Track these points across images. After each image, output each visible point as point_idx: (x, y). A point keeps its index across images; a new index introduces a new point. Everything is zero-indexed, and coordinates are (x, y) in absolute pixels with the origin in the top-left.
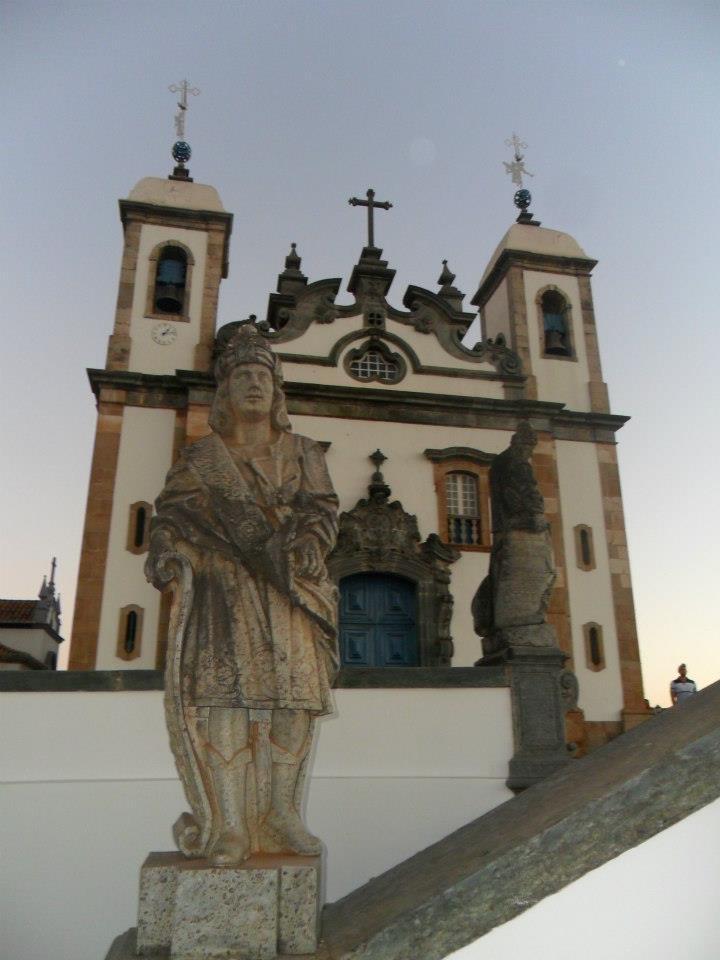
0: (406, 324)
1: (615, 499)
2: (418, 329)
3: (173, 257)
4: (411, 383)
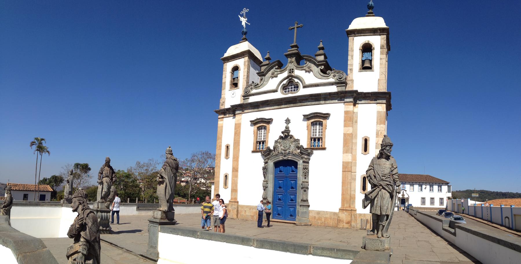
0: (302, 70)
2: (306, 71)
4: (302, 92)
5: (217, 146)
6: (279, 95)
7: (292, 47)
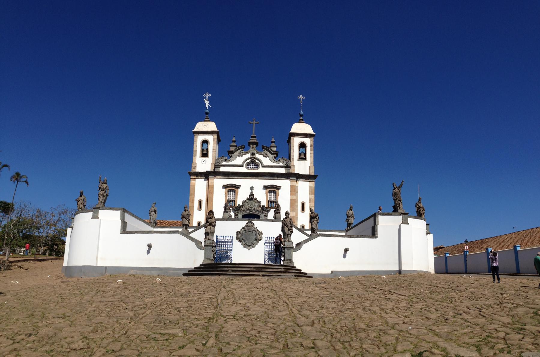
1: (312, 195)
2: (264, 156)
4: (261, 170)
5: (190, 200)
6: (244, 170)
7: (252, 137)
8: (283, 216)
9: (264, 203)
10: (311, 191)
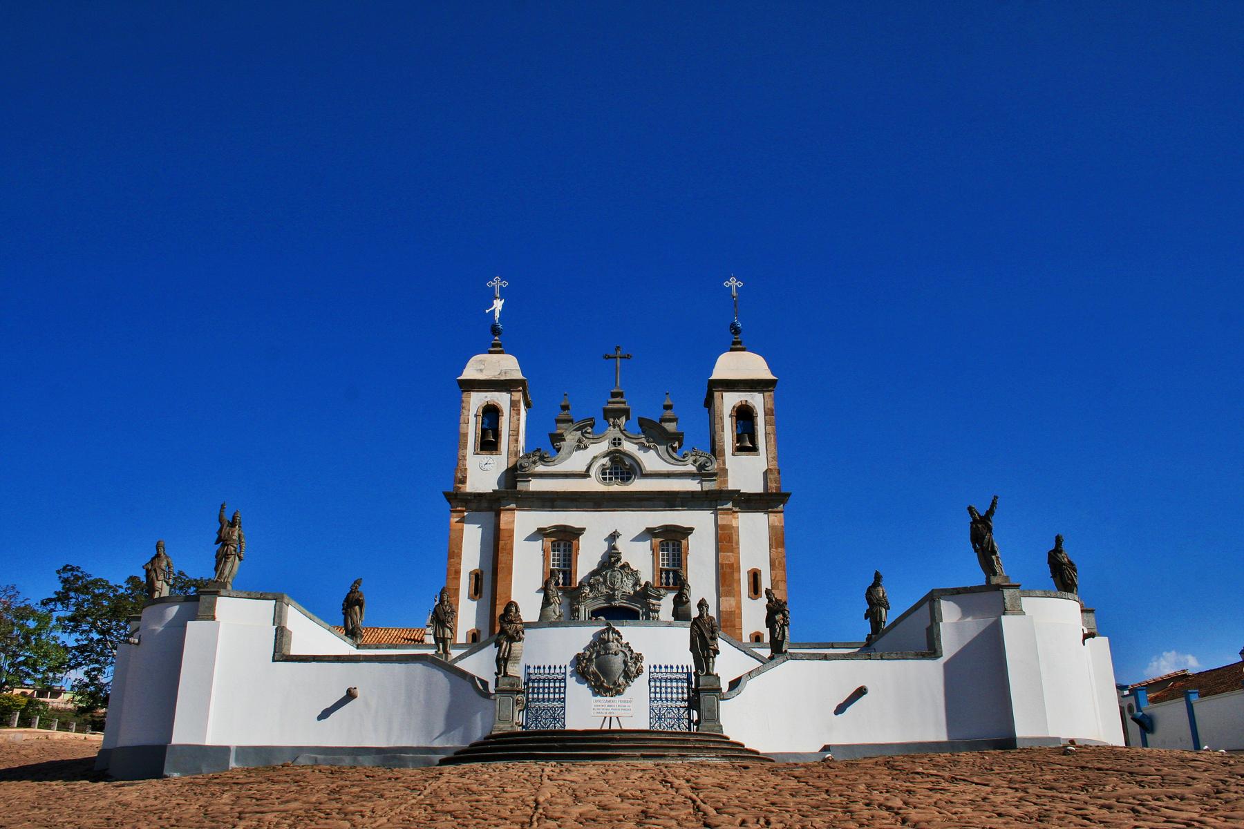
1: (780, 549)
3: (491, 413)
4: (638, 485)
7: (614, 395)
8: (695, 613)
9: (646, 576)
10: (776, 539)
